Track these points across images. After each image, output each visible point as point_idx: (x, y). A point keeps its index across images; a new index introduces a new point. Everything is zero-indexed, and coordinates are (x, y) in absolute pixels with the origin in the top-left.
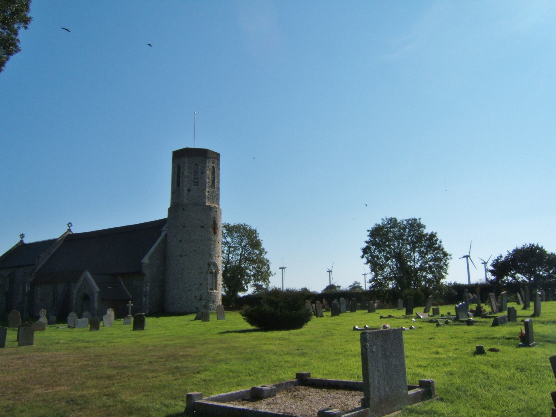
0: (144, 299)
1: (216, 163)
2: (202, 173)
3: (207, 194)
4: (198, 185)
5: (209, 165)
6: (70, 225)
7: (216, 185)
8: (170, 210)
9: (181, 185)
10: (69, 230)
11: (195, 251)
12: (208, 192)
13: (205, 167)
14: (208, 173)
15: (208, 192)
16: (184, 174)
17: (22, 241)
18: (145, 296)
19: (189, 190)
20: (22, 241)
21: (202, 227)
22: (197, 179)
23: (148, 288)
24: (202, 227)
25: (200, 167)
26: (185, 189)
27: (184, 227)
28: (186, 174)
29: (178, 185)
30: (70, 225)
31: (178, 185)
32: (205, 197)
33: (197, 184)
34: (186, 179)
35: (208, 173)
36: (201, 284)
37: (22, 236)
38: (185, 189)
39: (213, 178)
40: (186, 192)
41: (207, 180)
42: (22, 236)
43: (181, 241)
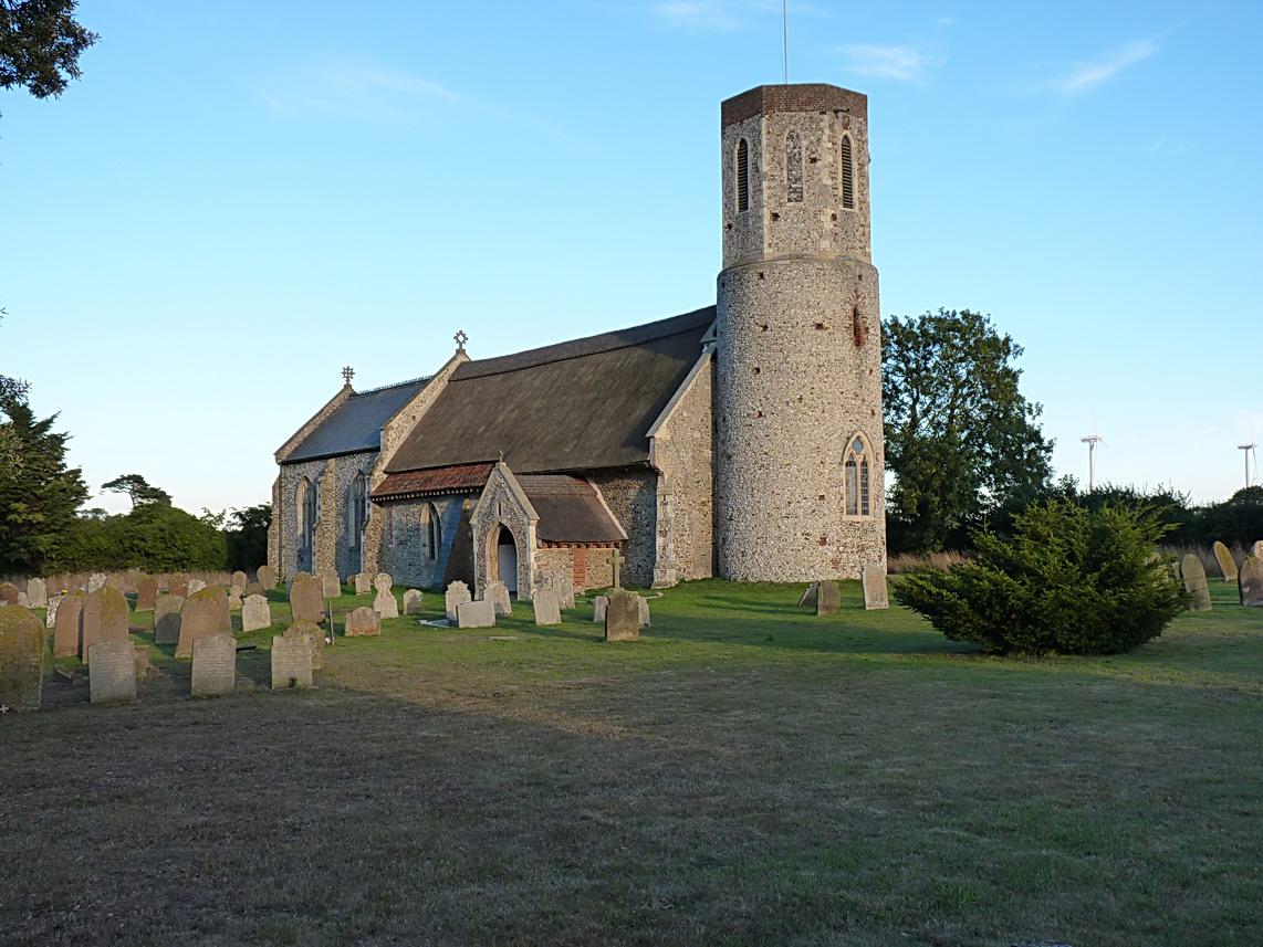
1: (855, 125)
2: (814, 160)
4: (799, 199)
6: (461, 337)
7: (856, 196)
8: (722, 281)
9: (751, 204)
10: (460, 352)
16: (757, 170)
17: (348, 386)
19: (775, 216)
21: (819, 326)
22: (798, 179)
24: (819, 326)
25: (805, 143)
26: (766, 213)
27: (765, 328)
28: (765, 168)
29: (744, 206)
30: (461, 337)
31: (744, 206)
36: (822, 497)
37: (348, 373)
38: (766, 213)
40: (767, 220)
42: (348, 373)
43: (758, 370)
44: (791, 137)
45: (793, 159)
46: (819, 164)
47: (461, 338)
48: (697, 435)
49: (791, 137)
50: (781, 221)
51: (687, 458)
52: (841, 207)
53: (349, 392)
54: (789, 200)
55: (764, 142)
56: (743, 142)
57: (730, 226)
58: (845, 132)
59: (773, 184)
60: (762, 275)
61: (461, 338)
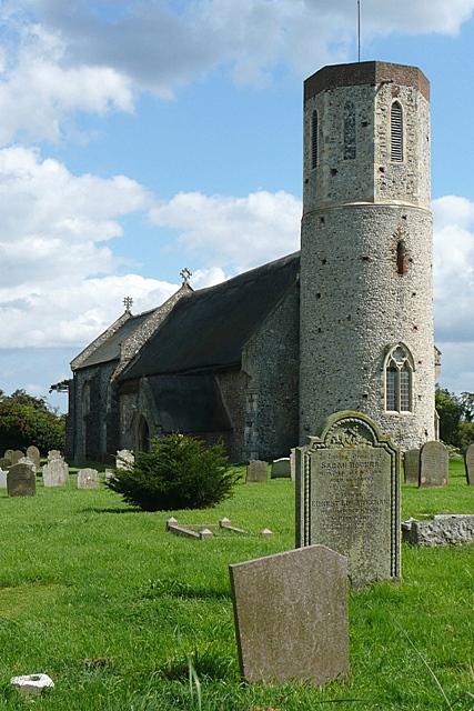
0: (247, 429)
2: (365, 124)
3: (377, 176)
5: (382, 102)
10: (186, 286)
11: (349, 318)
12: (382, 170)
13: (371, 108)
14: (381, 121)
15: (382, 170)
16: (322, 134)
17: (128, 312)
18: (250, 424)
19: (334, 172)
20: (128, 312)
22: (352, 141)
23: (255, 405)
25: (358, 110)
26: (326, 169)
27: (324, 262)
28: (326, 133)
32: (371, 186)
33: (351, 153)
34: (326, 146)
35: (377, 121)
36: (365, 396)
37: (128, 302)
39: (397, 133)
40: (327, 176)
41: (377, 141)
43: (319, 296)
44: (347, 107)
45: (349, 124)
46: (369, 127)
47: (186, 274)
48: (282, 347)
49: (347, 107)
50: (338, 176)
51: (273, 365)
52: (389, 161)
53: (128, 317)
54: (345, 158)
55: (327, 112)
56: (315, 112)
57: (306, 182)
58: (395, 99)
59: (333, 146)
60: (322, 220)
61: (186, 274)
